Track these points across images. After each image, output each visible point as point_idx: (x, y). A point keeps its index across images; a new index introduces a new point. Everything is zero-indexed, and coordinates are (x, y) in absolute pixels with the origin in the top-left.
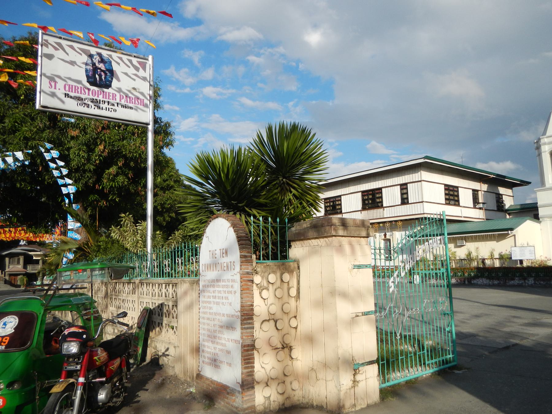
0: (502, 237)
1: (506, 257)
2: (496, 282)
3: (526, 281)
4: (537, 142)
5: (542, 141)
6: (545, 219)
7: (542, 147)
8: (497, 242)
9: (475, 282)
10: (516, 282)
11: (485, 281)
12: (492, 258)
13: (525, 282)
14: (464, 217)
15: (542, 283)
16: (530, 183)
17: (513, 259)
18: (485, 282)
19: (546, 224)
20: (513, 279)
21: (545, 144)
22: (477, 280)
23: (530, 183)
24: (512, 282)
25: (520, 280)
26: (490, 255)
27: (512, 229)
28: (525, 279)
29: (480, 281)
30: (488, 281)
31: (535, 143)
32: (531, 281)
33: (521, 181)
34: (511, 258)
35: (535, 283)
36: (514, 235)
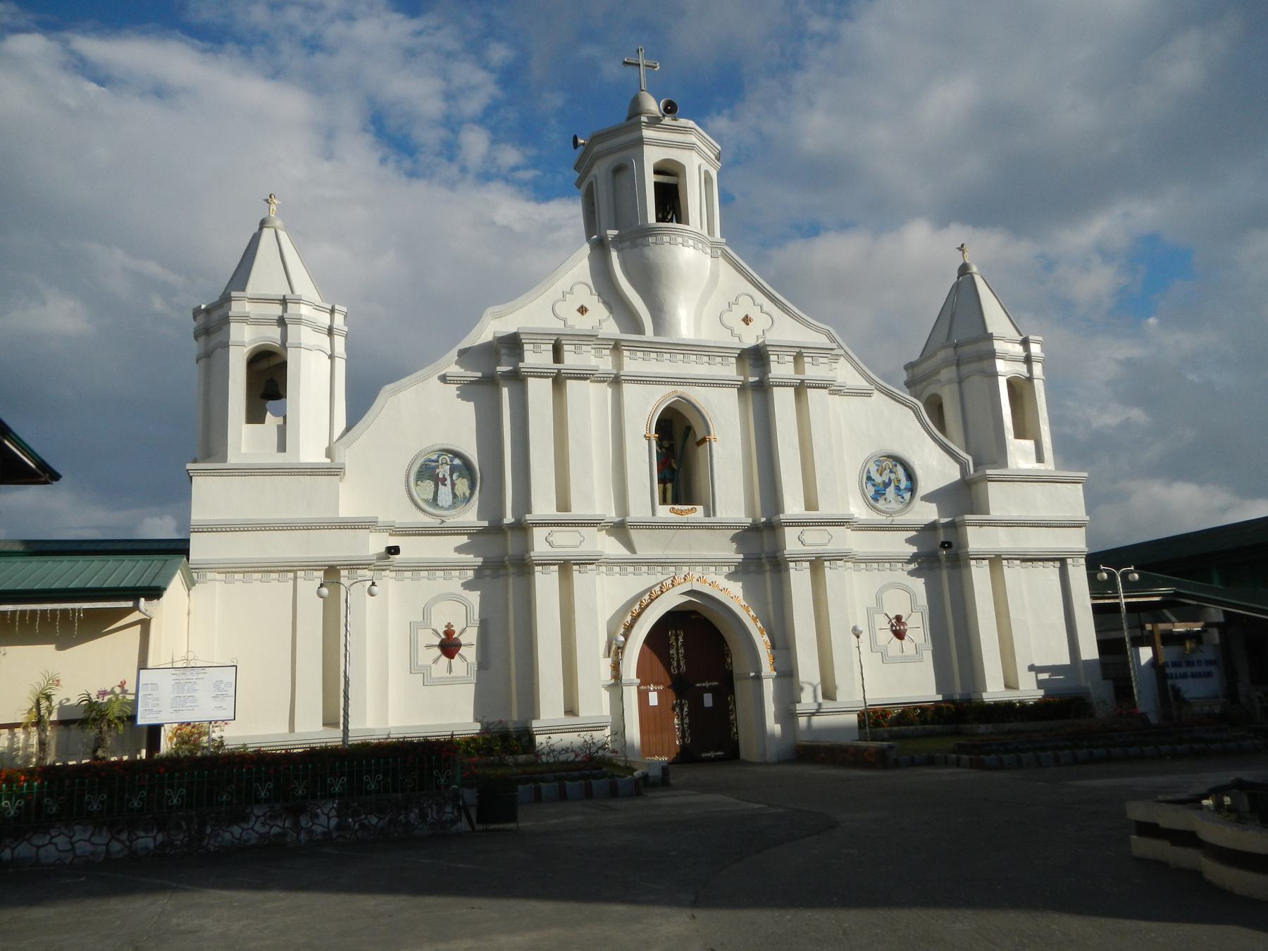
0: (96, 625)
1: (115, 711)
2: (146, 841)
3: (304, 821)
4: (207, 311)
5: (236, 308)
6: (210, 575)
7: (234, 328)
8: (61, 647)
9: (24, 849)
10: (257, 826)
11: (84, 841)
12: (39, 723)
13: (296, 824)
15: (374, 820)
16: (55, 477)
17: (140, 721)
18: (83, 847)
19: (213, 590)
20: (239, 817)
21: (245, 319)
22: (38, 840)
23: (55, 477)
24: (237, 830)
25: (273, 818)
26: (30, 704)
27: (155, 593)
28: (296, 811)
29: (54, 845)
30: (101, 839)
31: (197, 312)
32: (325, 818)
33: (42, 465)
34: (133, 718)
35: (339, 827)
36: (145, 624)
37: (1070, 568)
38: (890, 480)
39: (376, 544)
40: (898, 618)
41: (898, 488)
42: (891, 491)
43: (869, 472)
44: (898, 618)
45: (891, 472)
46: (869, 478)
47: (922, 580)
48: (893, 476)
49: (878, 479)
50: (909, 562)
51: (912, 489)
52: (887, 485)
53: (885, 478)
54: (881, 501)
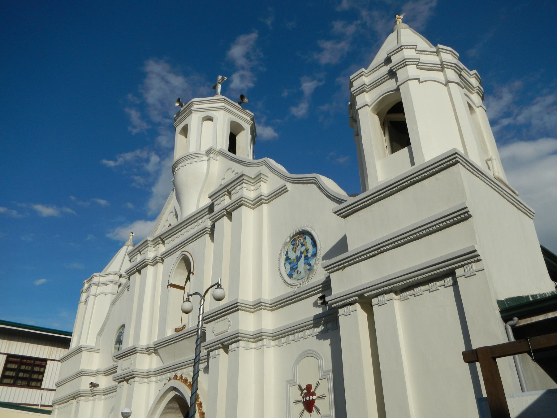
14: (42, 406)
37: (461, 281)
38: (301, 253)
39: (84, 384)
40: (309, 387)
41: (306, 258)
42: (301, 265)
43: (287, 253)
44: (309, 387)
45: (303, 245)
46: (288, 259)
47: (328, 341)
48: (303, 249)
49: (293, 256)
50: (316, 325)
51: (315, 255)
52: (298, 259)
53: (298, 253)
54: (295, 275)
